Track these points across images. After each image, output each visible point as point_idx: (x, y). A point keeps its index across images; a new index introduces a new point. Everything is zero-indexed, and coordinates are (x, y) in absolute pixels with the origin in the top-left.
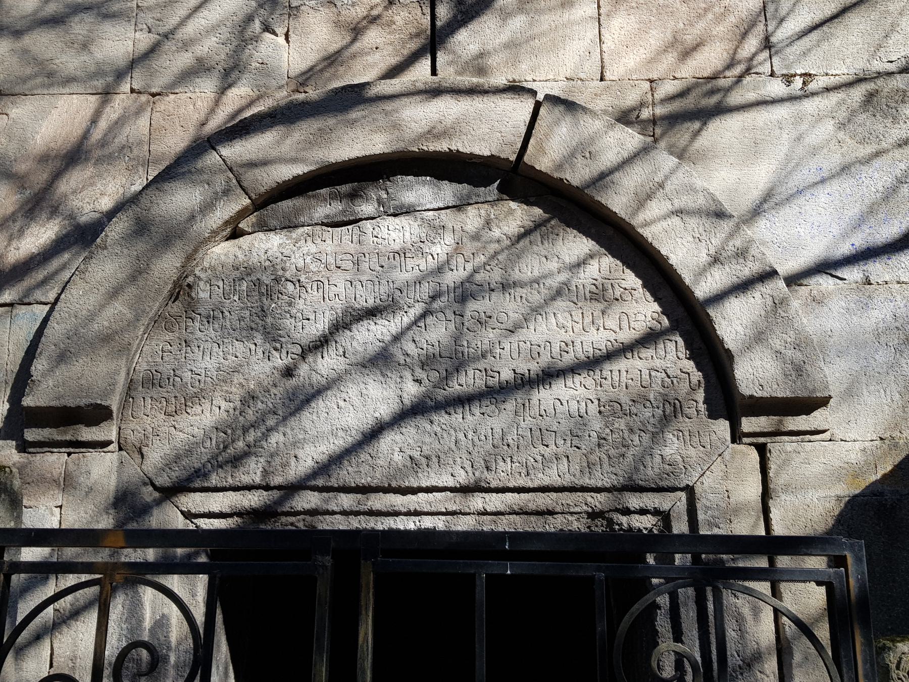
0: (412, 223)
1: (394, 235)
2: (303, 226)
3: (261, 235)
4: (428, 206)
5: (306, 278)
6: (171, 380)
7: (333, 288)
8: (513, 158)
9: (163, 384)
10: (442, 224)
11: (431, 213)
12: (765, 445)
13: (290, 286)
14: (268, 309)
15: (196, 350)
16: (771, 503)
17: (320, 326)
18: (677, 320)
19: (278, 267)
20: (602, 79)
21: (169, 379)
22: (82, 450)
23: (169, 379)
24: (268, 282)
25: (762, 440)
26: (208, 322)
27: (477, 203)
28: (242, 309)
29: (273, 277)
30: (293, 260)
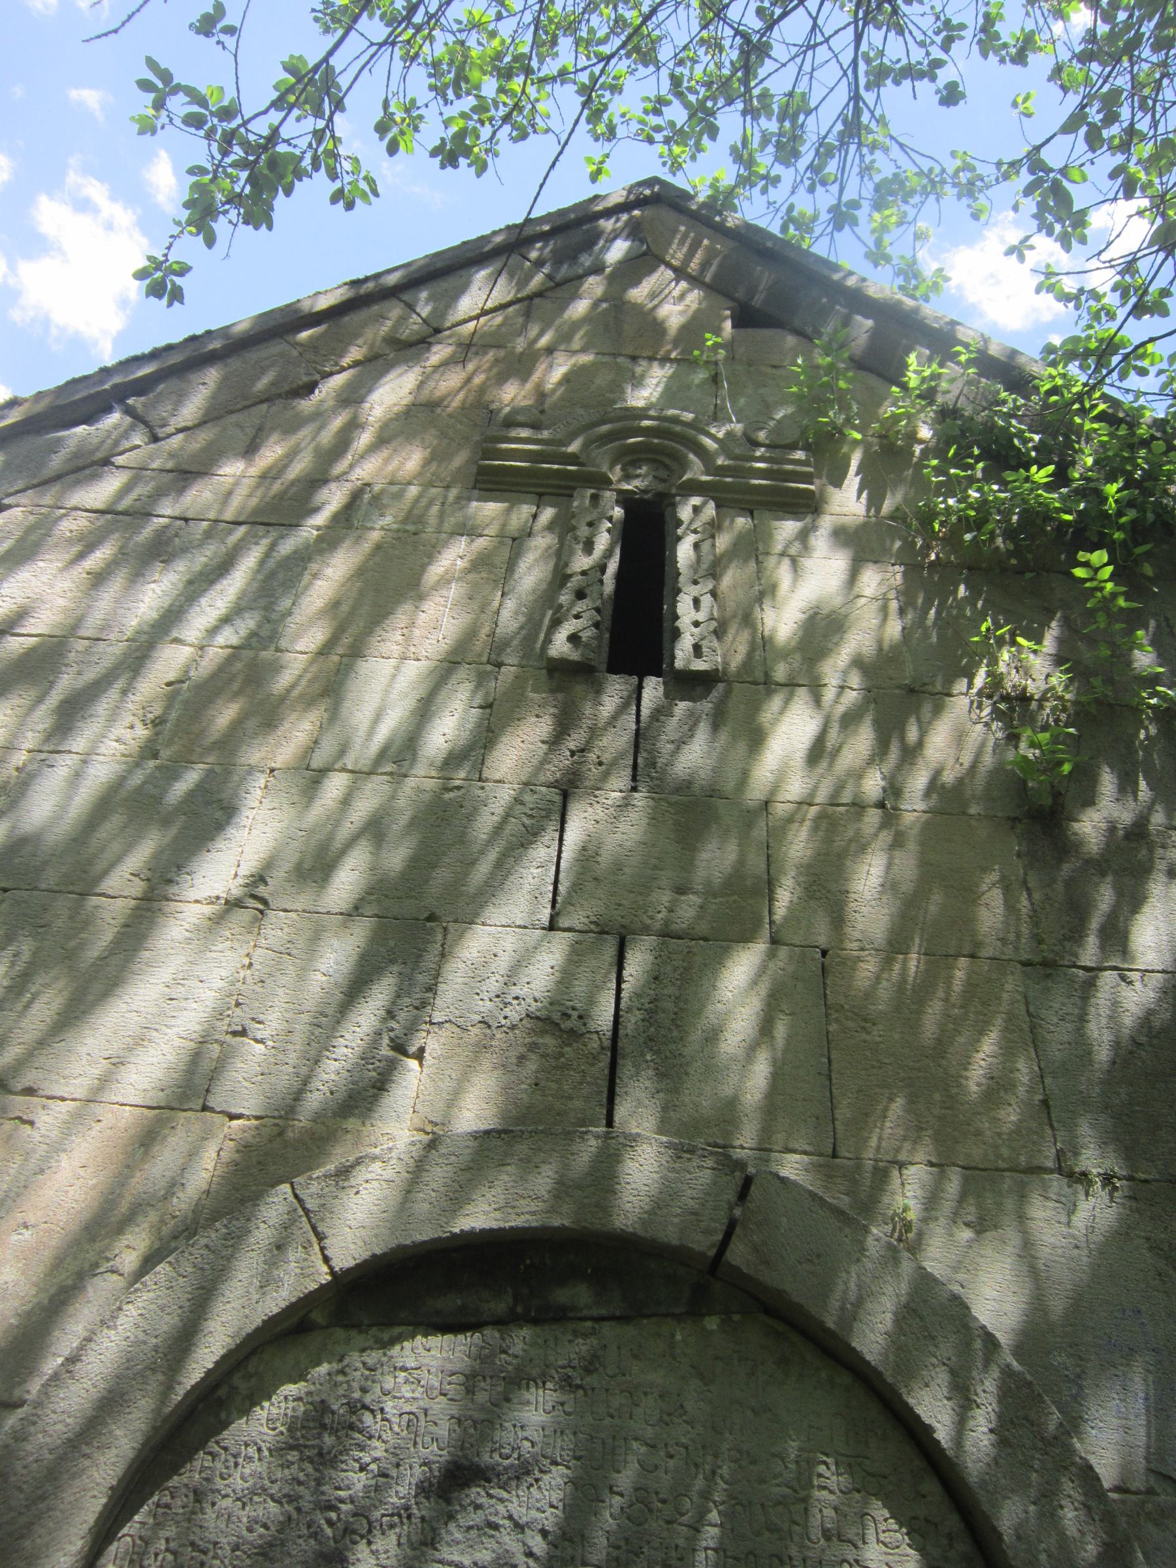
2: (400, 1324)
3: (339, 1333)
4: (585, 1313)
5: (394, 1407)
6: (160, 1558)
7: (433, 1428)
8: (712, 1253)
11: (589, 1324)
14: (329, 1453)
20: (834, 1155)
23: (156, 1555)
27: (654, 1315)
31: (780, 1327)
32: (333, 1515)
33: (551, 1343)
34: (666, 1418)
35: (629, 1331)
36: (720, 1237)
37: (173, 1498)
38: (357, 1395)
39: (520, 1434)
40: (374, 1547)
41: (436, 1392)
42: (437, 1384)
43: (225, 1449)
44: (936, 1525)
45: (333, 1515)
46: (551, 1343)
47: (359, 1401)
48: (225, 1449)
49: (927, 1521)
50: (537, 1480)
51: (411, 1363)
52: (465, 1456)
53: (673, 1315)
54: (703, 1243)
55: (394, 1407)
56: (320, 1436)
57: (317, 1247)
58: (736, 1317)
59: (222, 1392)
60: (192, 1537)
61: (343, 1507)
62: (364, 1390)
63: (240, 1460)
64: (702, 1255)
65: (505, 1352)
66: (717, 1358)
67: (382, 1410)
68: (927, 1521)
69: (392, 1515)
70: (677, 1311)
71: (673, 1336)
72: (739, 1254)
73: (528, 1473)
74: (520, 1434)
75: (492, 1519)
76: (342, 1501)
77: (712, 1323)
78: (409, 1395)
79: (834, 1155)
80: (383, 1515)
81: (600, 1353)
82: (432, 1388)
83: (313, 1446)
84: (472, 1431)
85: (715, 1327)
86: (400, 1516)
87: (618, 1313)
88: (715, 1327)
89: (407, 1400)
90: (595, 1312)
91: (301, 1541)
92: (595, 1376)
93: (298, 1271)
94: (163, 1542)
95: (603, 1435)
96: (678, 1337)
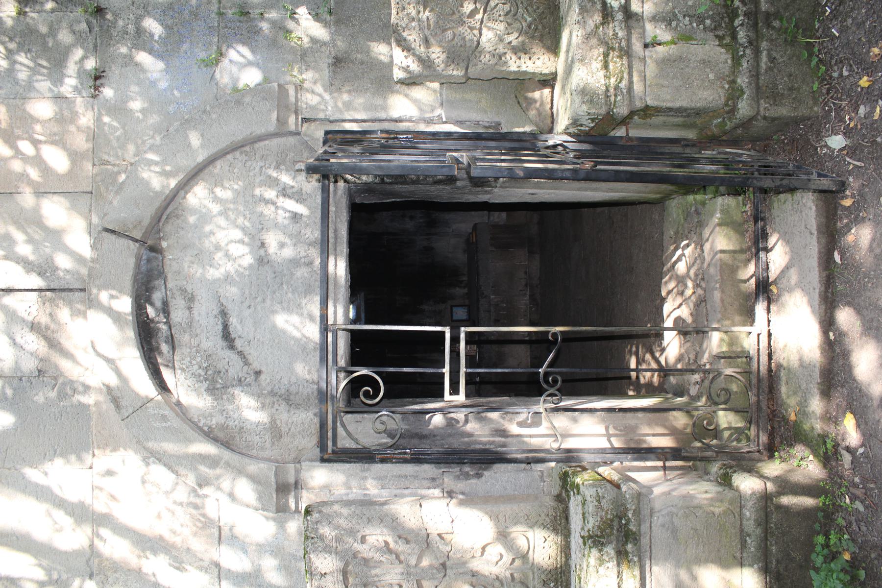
1: (180, 313)
13: (210, 372)
16: (331, 119)
25: (300, 119)
31: (164, 217)
35: (170, 276)
38: (202, 378)
59: (206, 429)
62: (200, 375)
77: (164, 244)
79: (92, 193)
90: (164, 290)
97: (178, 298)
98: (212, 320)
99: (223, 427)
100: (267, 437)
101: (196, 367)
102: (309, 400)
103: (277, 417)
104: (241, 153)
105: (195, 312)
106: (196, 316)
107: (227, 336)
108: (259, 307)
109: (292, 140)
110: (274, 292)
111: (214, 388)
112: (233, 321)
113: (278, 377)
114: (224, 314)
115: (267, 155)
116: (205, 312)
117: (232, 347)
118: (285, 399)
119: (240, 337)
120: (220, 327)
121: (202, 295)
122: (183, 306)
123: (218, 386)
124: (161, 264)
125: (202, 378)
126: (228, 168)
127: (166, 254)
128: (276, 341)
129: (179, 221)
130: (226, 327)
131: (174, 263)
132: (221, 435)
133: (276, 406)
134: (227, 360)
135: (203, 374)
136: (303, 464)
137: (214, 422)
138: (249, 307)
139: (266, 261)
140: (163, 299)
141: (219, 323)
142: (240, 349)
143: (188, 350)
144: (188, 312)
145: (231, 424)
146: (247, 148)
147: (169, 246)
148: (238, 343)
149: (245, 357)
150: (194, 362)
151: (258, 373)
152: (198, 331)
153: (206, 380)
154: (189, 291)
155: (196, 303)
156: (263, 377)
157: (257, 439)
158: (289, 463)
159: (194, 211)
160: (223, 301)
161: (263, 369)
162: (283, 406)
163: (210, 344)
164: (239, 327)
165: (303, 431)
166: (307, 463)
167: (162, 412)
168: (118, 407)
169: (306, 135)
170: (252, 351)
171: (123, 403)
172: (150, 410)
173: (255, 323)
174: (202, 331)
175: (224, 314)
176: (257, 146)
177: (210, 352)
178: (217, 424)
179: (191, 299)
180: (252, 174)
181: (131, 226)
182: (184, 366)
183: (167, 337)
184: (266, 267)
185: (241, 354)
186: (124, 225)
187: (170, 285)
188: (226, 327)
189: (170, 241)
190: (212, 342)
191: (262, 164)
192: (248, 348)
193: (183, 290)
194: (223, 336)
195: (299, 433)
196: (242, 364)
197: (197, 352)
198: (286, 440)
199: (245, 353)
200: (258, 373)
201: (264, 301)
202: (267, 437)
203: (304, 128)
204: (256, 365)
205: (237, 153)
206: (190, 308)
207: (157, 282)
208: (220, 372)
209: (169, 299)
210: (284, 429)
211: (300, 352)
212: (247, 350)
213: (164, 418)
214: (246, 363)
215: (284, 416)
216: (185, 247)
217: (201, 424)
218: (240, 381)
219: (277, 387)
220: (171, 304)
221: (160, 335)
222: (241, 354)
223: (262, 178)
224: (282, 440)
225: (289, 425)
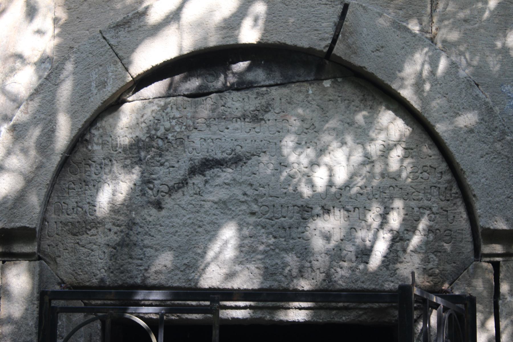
0: (250, 96)
1: (238, 105)
4: (262, 83)
5: (172, 136)
6: (75, 210)
7: (192, 144)
8: (325, 50)
9: (69, 212)
10: (273, 97)
11: (264, 89)
12: (498, 262)
13: (160, 142)
15: (92, 188)
17: (182, 172)
18: (441, 173)
19: (151, 128)
21: (73, 209)
22: (14, 259)
23: (73, 209)
24: (143, 139)
26: (101, 168)
27: (298, 82)
28: (126, 159)
29: (148, 135)
30: (162, 123)
32: (151, 186)
33: (246, 100)
34: (306, 131)
35: (285, 91)
36: (329, 42)
37: (74, 185)
38: (153, 132)
39: (236, 143)
40: (173, 197)
41: (191, 128)
42: (192, 124)
43: (94, 162)
44: (435, 169)
45: (151, 186)
46: (246, 100)
47: (155, 135)
48: (94, 162)
49: (430, 166)
50: (245, 163)
51: (178, 115)
52: (210, 155)
53: (307, 81)
54: (322, 46)
55: (172, 136)
56: (139, 152)
57: (120, 64)
58: (339, 80)
59: (88, 137)
60: (88, 201)
61: (156, 182)
62: (156, 130)
63: (103, 166)
64: (322, 51)
65: (224, 106)
66: (330, 100)
67: (167, 138)
68: (430, 166)
69: (179, 183)
70: (309, 79)
71: (308, 91)
72: (339, 50)
73: (240, 160)
74: (236, 143)
75: (226, 181)
76: (155, 179)
77: (327, 84)
78: (178, 130)
80: (175, 184)
81: (271, 102)
82: (189, 126)
83: (137, 157)
84: (212, 144)
85: (328, 85)
86: (183, 183)
87: (279, 83)
88: (328, 85)
89: (178, 133)
90: (267, 83)
91: (138, 197)
92: (269, 113)
93: (113, 77)
94: (75, 203)
95: (275, 141)
96: (310, 92)
97: (257, 101)
98: (228, 146)
99: (88, 160)
100: (74, 216)
101: (167, 125)
102: (122, 272)
103: (100, 229)
104: (449, 182)
105: (239, 124)
106: (232, 126)
107: (206, 166)
108: (244, 207)
109: (469, 248)
110: (264, 227)
111: (140, 148)
112: (227, 174)
113: (153, 232)
114: (237, 160)
115: (447, 217)
116: (238, 135)
117: (193, 171)
118: (123, 240)
119: (206, 182)
120: (219, 156)
121: (263, 132)
122: (247, 107)
123: (143, 154)
124: (301, 79)
125: (153, 132)
126: (428, 164)
127: (315, 85)
128: (199, 230)
129: (357, 102)
130: (220, 163)
131: (302, 97)
132: (78, 157)
133: (115, 229)
134: (177, 165)
135: (159, 134)
136: (37, 262)
137: (96, 147)
138: (245, 194)
139: (306, 215)
140: (256, 82)
141: (225, 155)
142: (190, 182)
143: (189, 115)
144: (239, 115)
145: (93, 169)
146: (455, 189)
147: (325, 89)
148: (198, 180)
149: (179, 188)
150: (174, 122)
151: (159, 206)
152: (214, 128)
153: (151, 138)
154: (267, 116)
155: (251, 125)
156: (153, 211)
157: (72, 202)
158: (39, 246)
159: (370, 121)
160: (254, 160)
161: (163, 213)
162: (114, 238)
163: (198, 144)
164: (218, 181)
165: (81, 264)
166: (38, 269)
167: (110, 82)
168: (118, 26)
169: (476, 267)
170: (187, 198)
171: (122, 33)
172: (113, 68)
173: (224, 203)
174: (215, 133)
175: (237, 160)
176: (459, 202)
177: (186, 143)
178: (93, 152)
179: (256, 118)
180: (421, 195)
181: (350, 41)
182: (169, 110)
183: (207, 87)
184: (297, 216)
185: (183, 183)
186: (351, 33)
187: (275, 92)
188: (220, 163)
189: (330, 91)
190: (201, 144)
191: (434, 210)
192: (191, 192)
193: (267, 108)
194: (207, 160)
195: (79, 259)
196: (171, 184)
197: (187, 127)
198: (70, 240)
199: (185, 189)
200: (159, 206)
201: (253, 214)
202: (74, 216)
203: (485, 265)
204: (168, 202)
205: (448, 177)
206: (244, 117)
207: (278, 74)
208: (161, 155)
209: (256, 90)
210: (84, 238)
211: (186, 262)
212: (189, 190)
213: (103, 84)
214: (172, 190)
215: (102, 239)
216: (323, 109)
217: (93, 131)
218: (149, 182)
219: (140, 230)
220: (249, 93)
221: (210, 78)
222: (183, 183)
223: (416, 209)
224: (70, 236)
225: (89, 246)
